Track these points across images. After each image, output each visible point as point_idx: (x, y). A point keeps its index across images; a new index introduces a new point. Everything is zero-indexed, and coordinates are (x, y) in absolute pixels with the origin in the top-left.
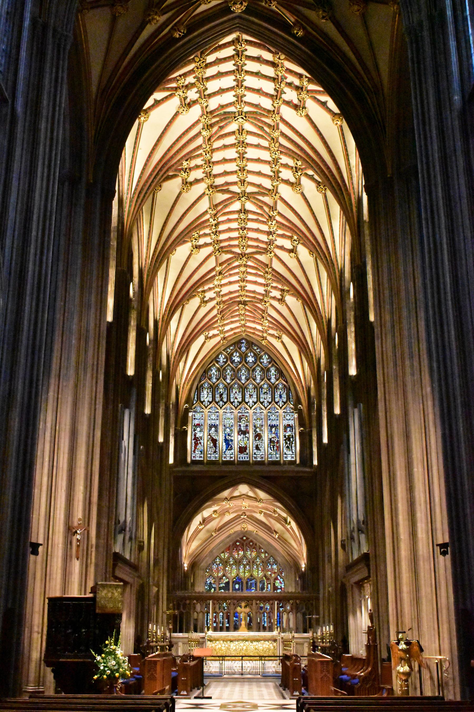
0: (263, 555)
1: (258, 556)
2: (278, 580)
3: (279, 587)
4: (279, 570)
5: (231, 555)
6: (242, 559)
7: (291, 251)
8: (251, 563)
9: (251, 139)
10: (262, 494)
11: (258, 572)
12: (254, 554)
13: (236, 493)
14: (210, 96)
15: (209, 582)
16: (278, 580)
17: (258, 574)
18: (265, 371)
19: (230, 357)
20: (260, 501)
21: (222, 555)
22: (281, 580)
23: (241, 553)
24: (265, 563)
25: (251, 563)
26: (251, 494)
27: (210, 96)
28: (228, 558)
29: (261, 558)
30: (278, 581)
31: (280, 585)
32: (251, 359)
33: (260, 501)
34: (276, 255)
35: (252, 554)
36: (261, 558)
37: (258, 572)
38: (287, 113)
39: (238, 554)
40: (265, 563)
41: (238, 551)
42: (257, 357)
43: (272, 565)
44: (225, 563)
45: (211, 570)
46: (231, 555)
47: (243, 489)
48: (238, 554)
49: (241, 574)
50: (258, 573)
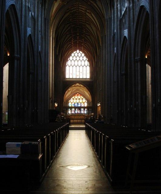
5: (75, 97)
7: (89, 35)
8: (79, 99)
9: (80, 5)
10: (82, 86)
13: (76, 85)
14: (72, 10)
18: (83, 57)
19: (74, 54)
20: (81, 87)
23: (77, 97)
24: (82, 99)
25: (79, 99)
26: (79, 85)
27: (72, 10)
32: (80, 55)
33: (81, 87)
34: (85, 36)
35: (79, 97)
38: (87, 14)
40: (82, 99)
42: (81, 54)
44: (73, 99)
46: (75, 97)
47: (78, 84)
50: (81, 101)
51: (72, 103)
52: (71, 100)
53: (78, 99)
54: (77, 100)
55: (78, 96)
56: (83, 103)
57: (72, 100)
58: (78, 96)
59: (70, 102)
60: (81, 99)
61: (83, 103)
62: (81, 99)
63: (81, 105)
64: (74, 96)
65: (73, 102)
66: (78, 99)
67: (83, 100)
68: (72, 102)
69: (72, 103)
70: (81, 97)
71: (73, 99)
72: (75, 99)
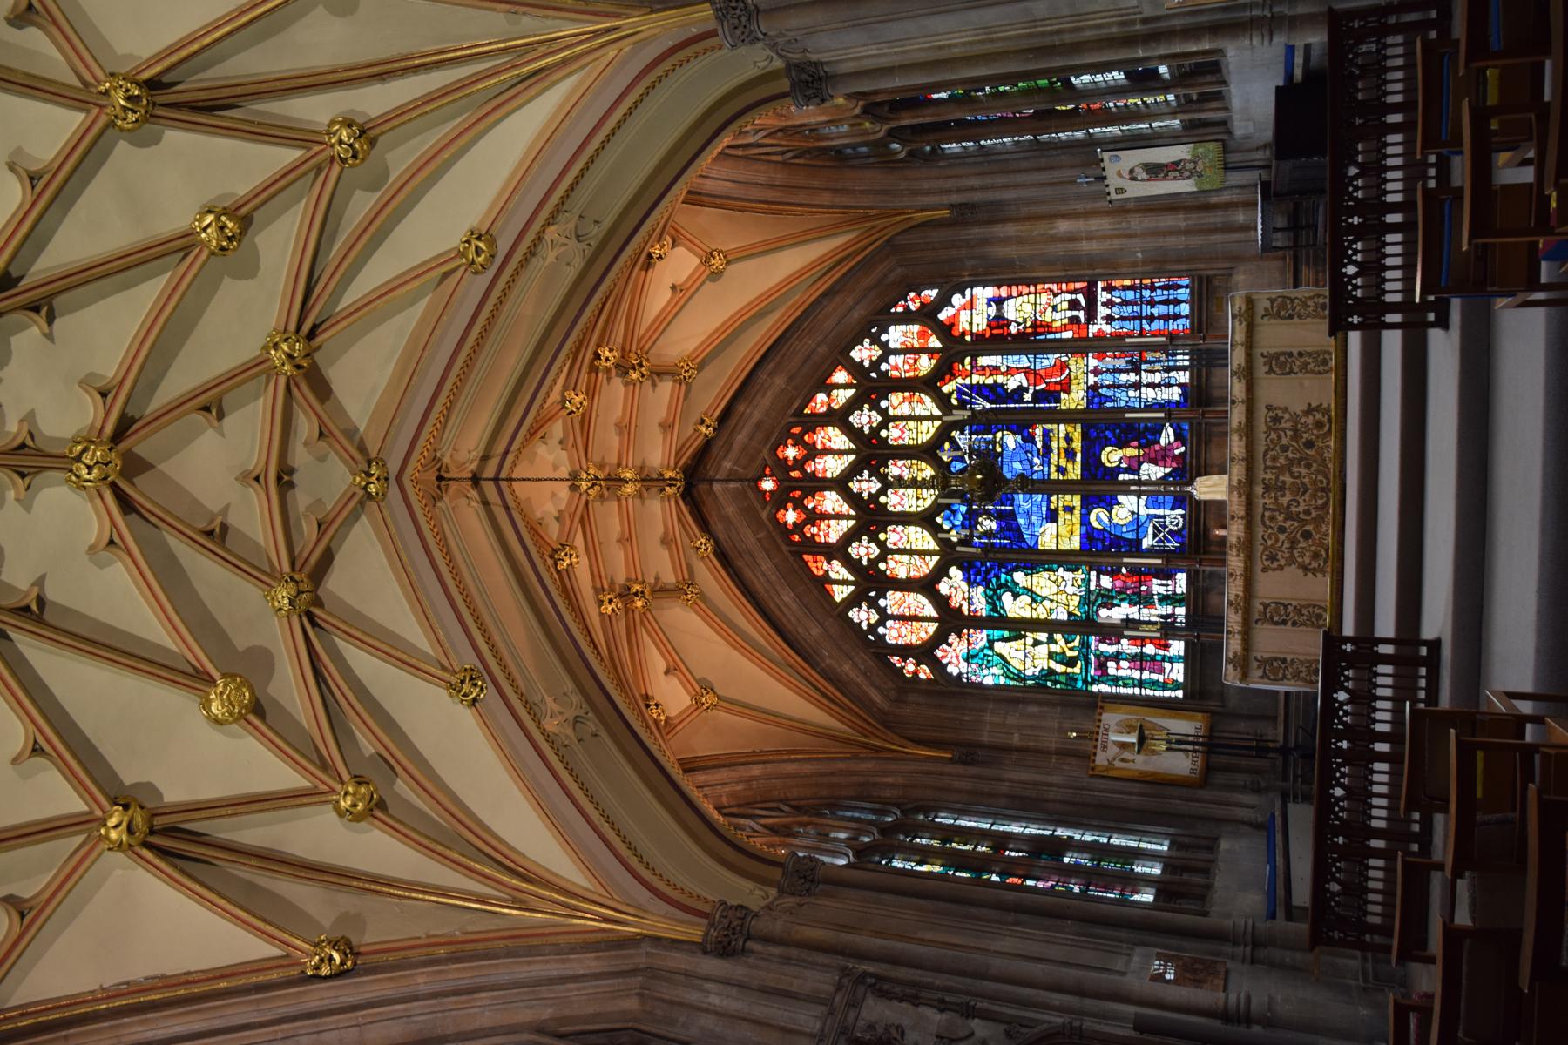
0: (842, 396)
1: (839, 418)
2: (956, 316)
3: (992, 311)
4: (907, 318)
5: (838, 551)
6: (853, 499)
8: (873, 452)
11: (920, 419)
12: (835, 438)
15: (963, 664)
16: (956, 316)
17: (932, 418)
21: (840, 593)
22: (957, 300)
23: (831, 501)
24: (873, 387)
25: (873, 452)
28: (851, 564)
29: (853, 405)
30: (964, 317)
31: (981, 305)
36: (853, 405)
37: (920, 419)
39: (838, 516)
40: (873, 387)
41: (815, 517)
43: (887, 352)
44: (872, 582)
45: (905, 651)
46: (838, 551)
48: (838, 516)
49: (928, 497)
51: (952, 620)
52: (893, 633)
53: (866, 485)
54: (896, 501)
55: (819, 484)
56: (945, 370)
57: (893, 601)
58: (819, 484)
59: (925, 652)
60: (864, 419)
61: (945, 370)
62: (864, 419)
63: (983, 424)
64: (819, 566)
65: (927, 586)
66: (866, 485)
67: (898, 366)
68: (920, 603)
69: (952, 620)
70: (839, 418)
71: (872, 582)
72: (863, 550)
